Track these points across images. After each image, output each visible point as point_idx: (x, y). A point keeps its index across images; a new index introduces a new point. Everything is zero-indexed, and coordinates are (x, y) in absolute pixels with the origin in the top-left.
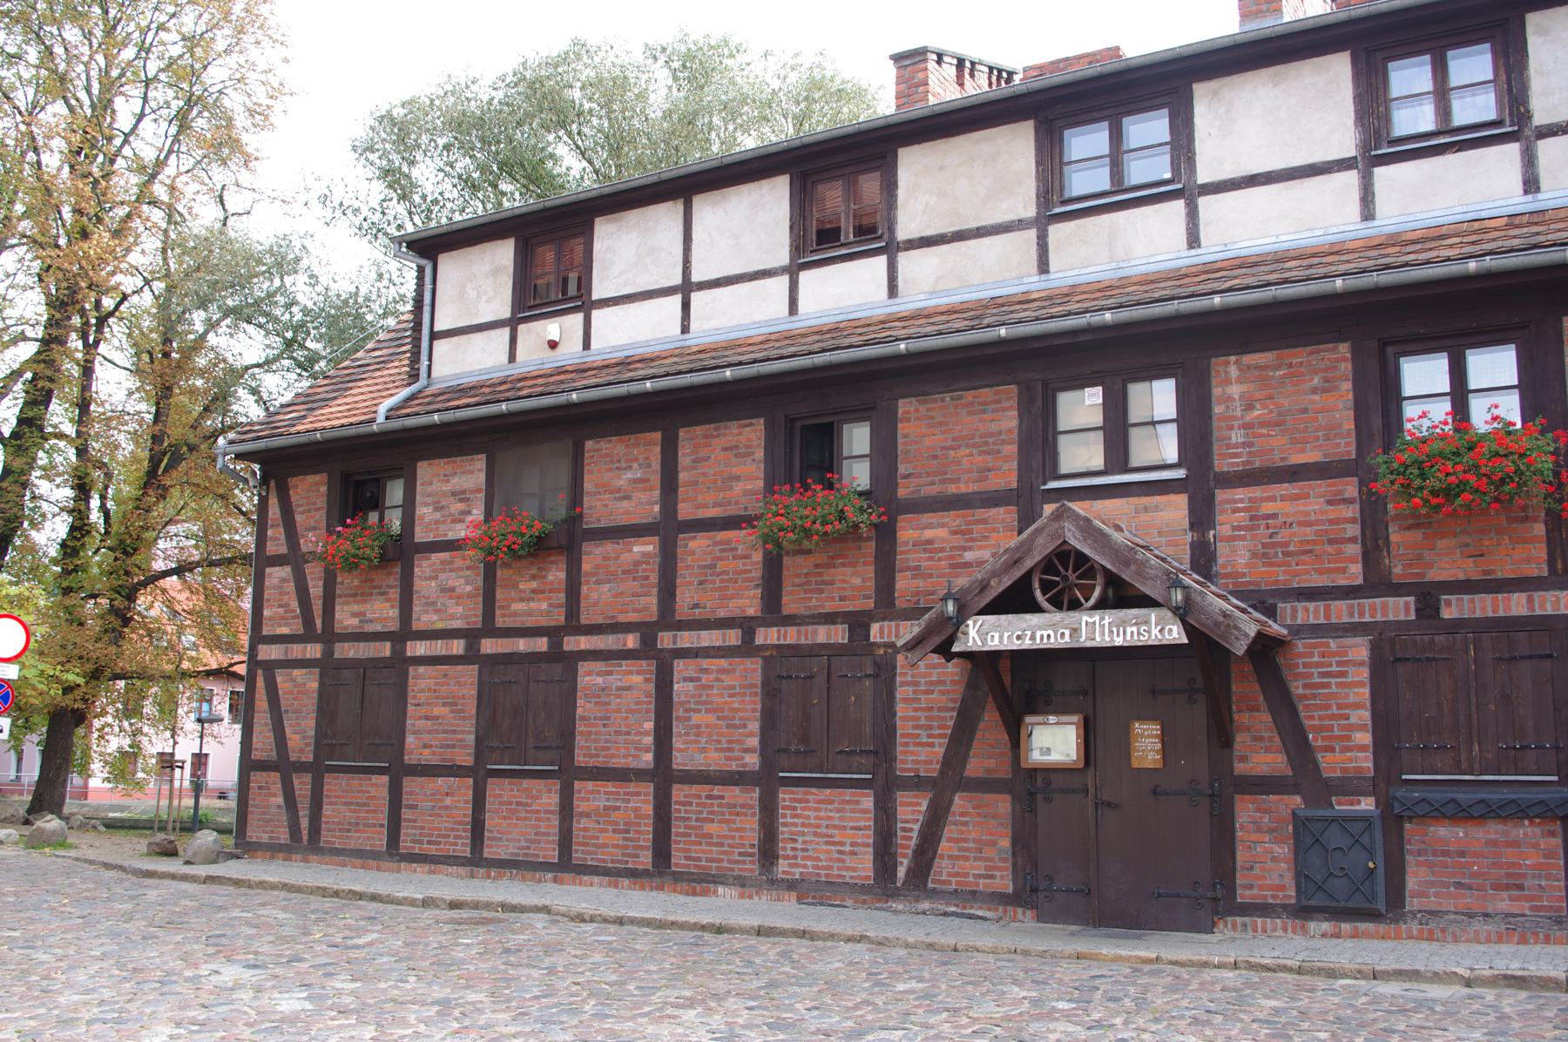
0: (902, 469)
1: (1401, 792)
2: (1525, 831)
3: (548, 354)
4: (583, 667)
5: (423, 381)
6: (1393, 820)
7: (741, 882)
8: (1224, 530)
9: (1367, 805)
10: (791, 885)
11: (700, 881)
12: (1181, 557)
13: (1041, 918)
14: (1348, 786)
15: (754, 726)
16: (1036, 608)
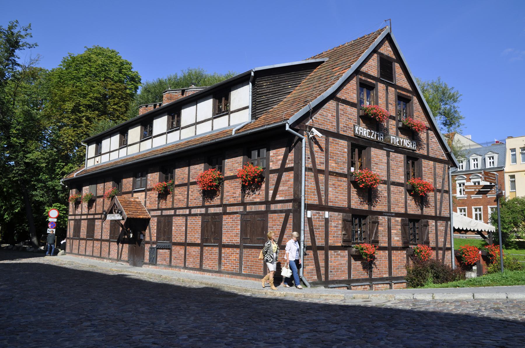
0: (123, 187)
1: (159, 244)
2: (167, 250)
3: (97, 163)
4: (96, 221)
5: (85, 168)
6: (157, 249)
7: (107, 259)
8: (147, 199)
9: (155, 246)
10: (110, 259)
11: (104, 258)
12: (143, 204)
13: (130, 265)
14: (154, 243)
15: (109, 231)
16: (113, 213)
